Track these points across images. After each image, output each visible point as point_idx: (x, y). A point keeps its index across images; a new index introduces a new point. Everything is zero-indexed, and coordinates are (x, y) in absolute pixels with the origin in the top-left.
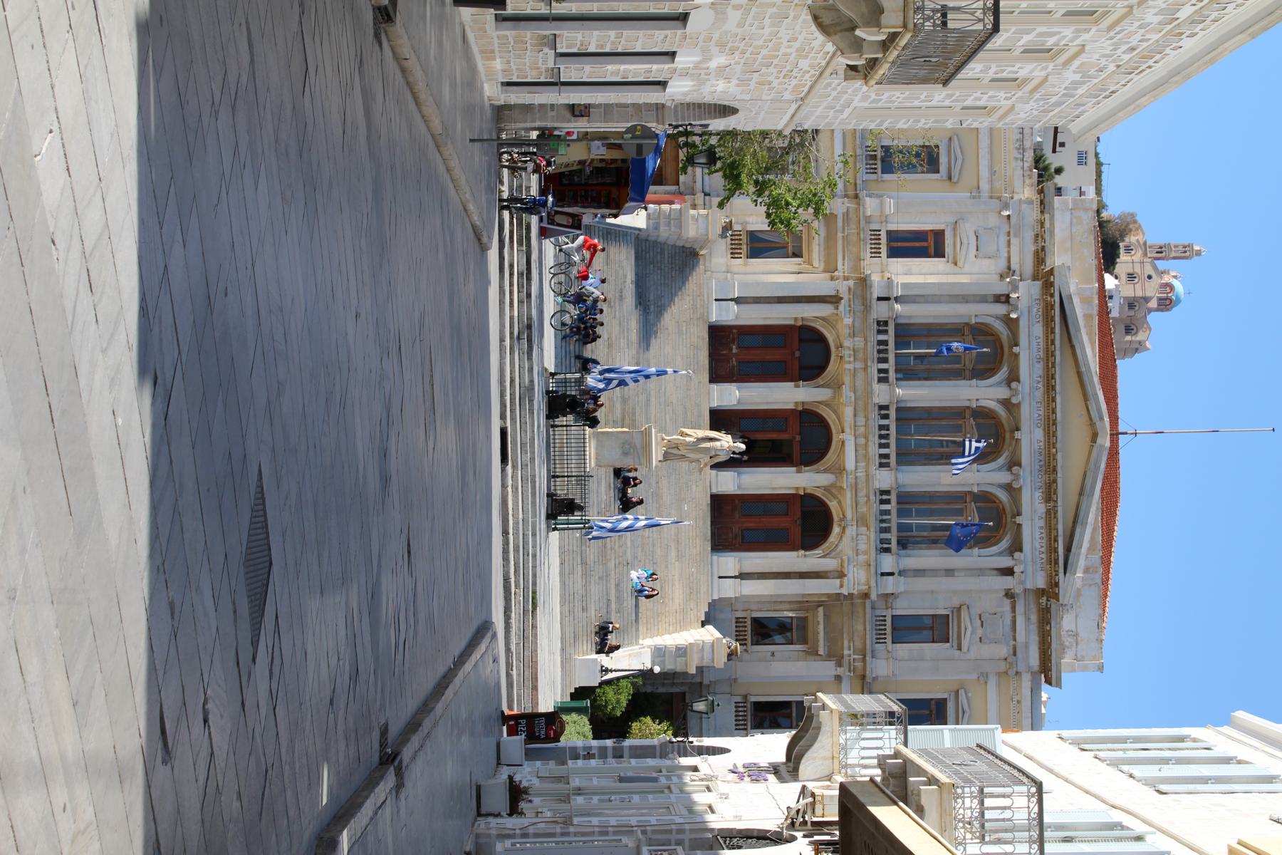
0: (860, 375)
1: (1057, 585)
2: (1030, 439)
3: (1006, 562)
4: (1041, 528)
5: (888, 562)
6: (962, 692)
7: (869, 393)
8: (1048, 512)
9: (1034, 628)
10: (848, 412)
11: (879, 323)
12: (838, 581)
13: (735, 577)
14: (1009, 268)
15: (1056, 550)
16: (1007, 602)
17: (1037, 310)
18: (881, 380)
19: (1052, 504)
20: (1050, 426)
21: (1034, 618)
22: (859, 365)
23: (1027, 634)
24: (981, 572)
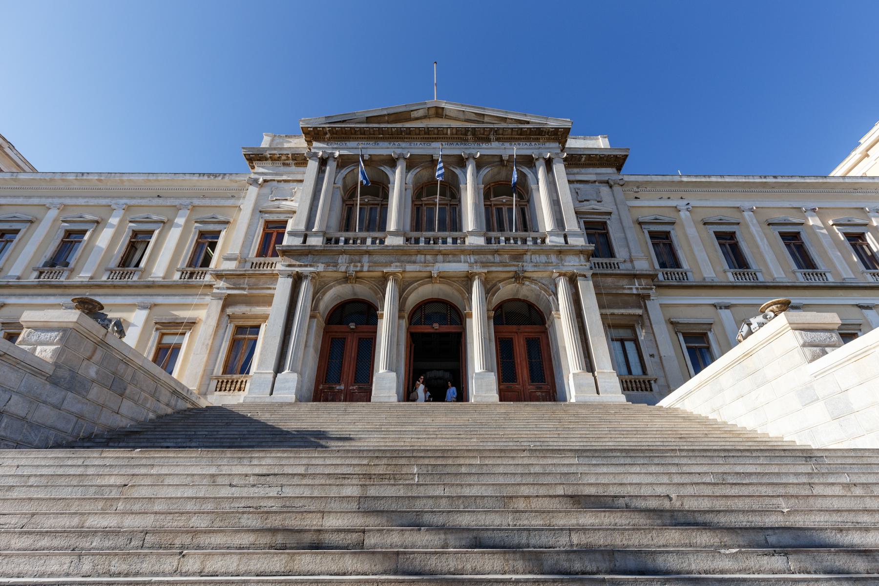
0: (376, 258)
6: (641, 220)
7: (396, 251)
8: (498, 140)
9: (583, 170)
13: (594, 375)
18: (382, 242)
19: (492, 137)
20: (429, 135)
21: (576, 170)
22: (365, 259)
23: (590, 174)
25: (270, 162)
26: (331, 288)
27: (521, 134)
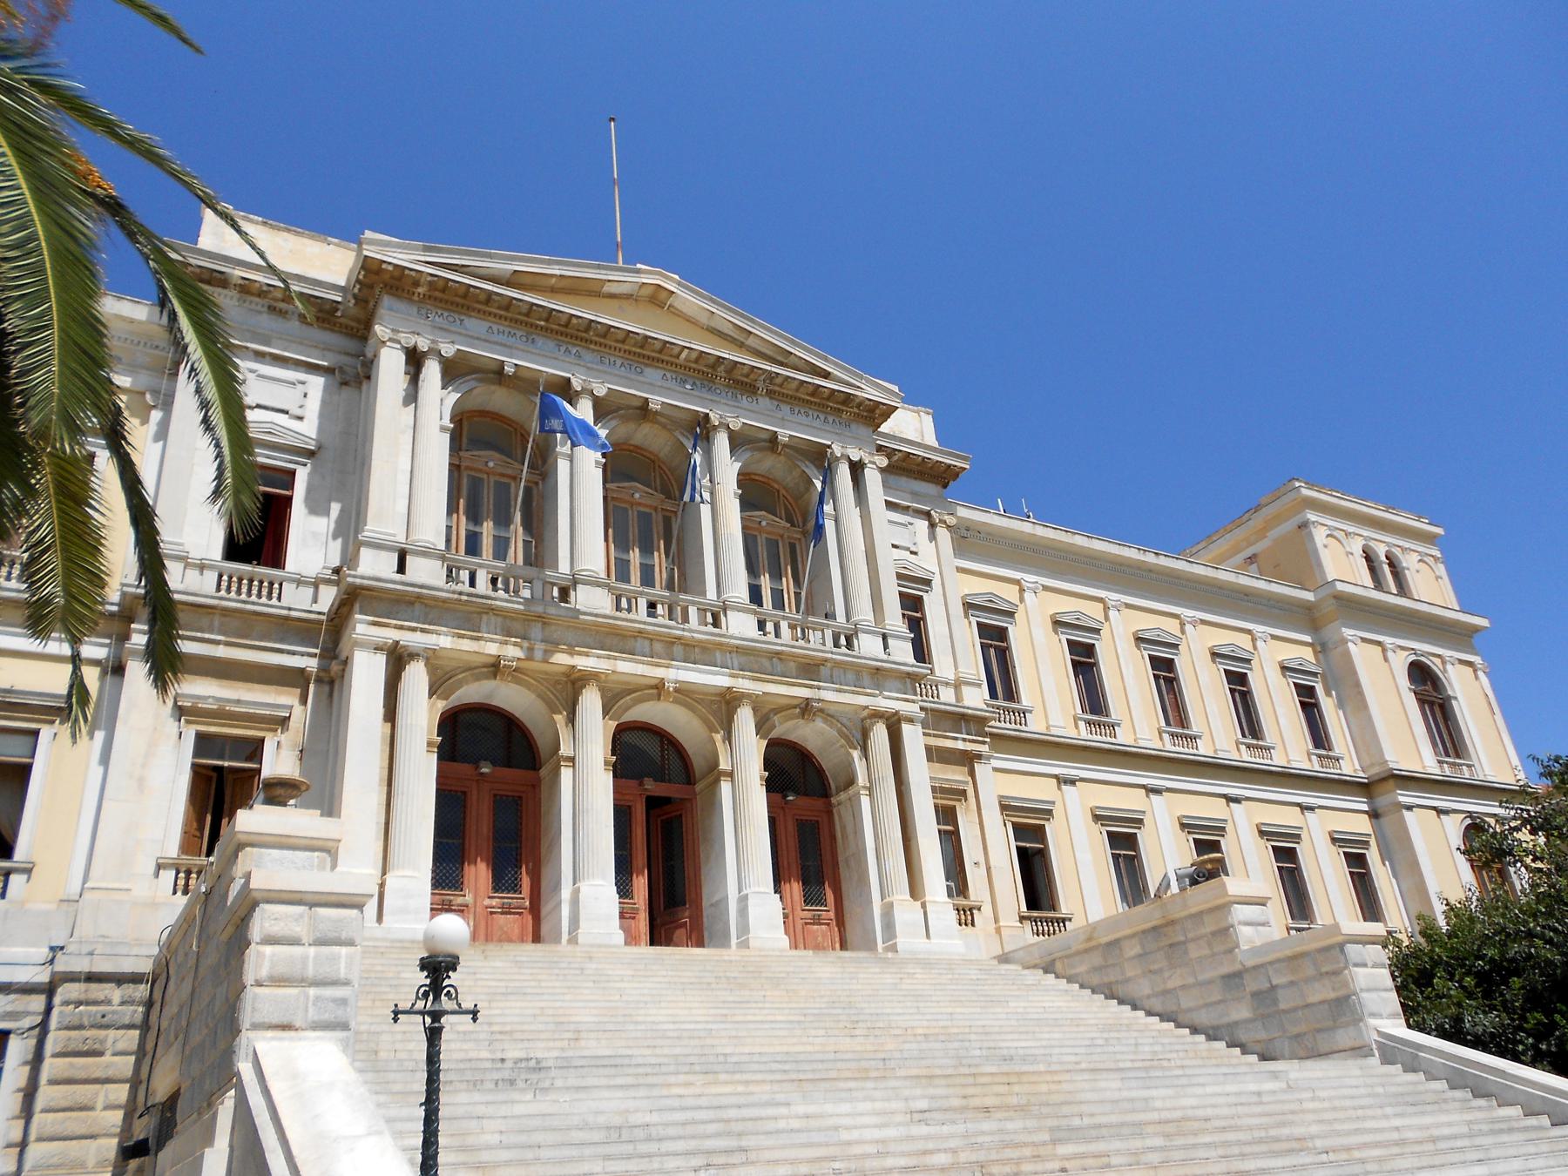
4: (792, 411)
8: (771, 394)
10: (627, 667)
12: (906, 729)
19: (760, 384)
25: (234, 293)
26: (460, 684)
27: (813, 394)
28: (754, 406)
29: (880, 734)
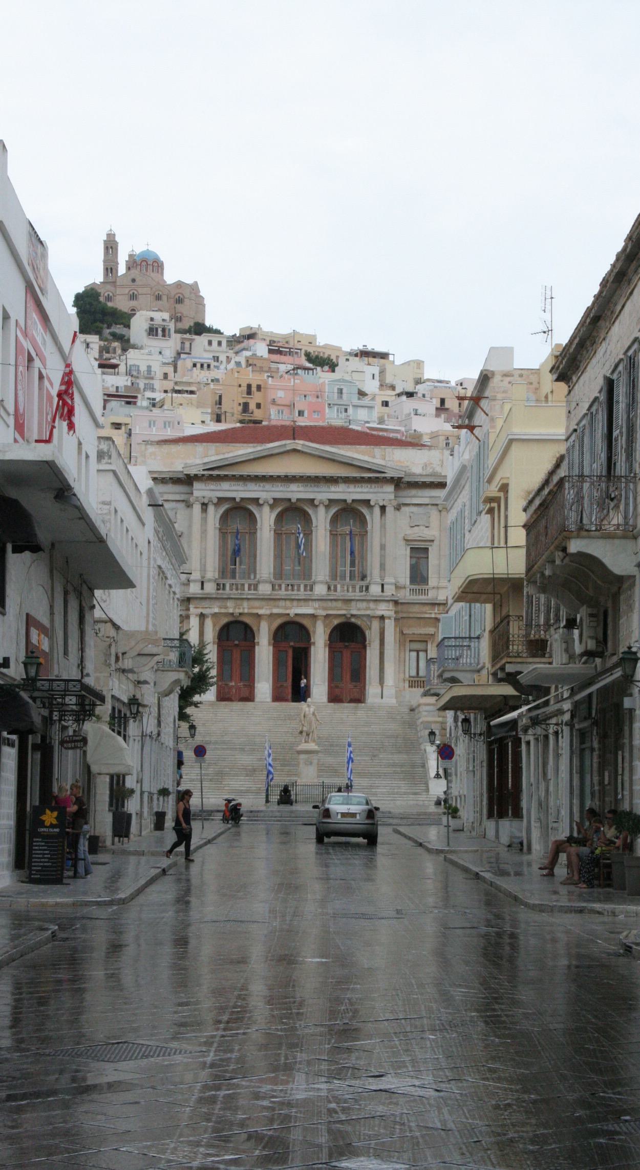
1: (392, 478)
2: (296, 492)
3: (377, 510)
5: (375, 590)
9: (420, 492)
10: (275, 611)
11: (218, 589)
12: (387, 621)
14: (183, 501)
15: (370, 478)
16: (403, 509)
17: (212, 486)
18: (256, 589)
23: (424, 496)
24: (383, 526)
28: (337, 489)
29: (376, 625)
